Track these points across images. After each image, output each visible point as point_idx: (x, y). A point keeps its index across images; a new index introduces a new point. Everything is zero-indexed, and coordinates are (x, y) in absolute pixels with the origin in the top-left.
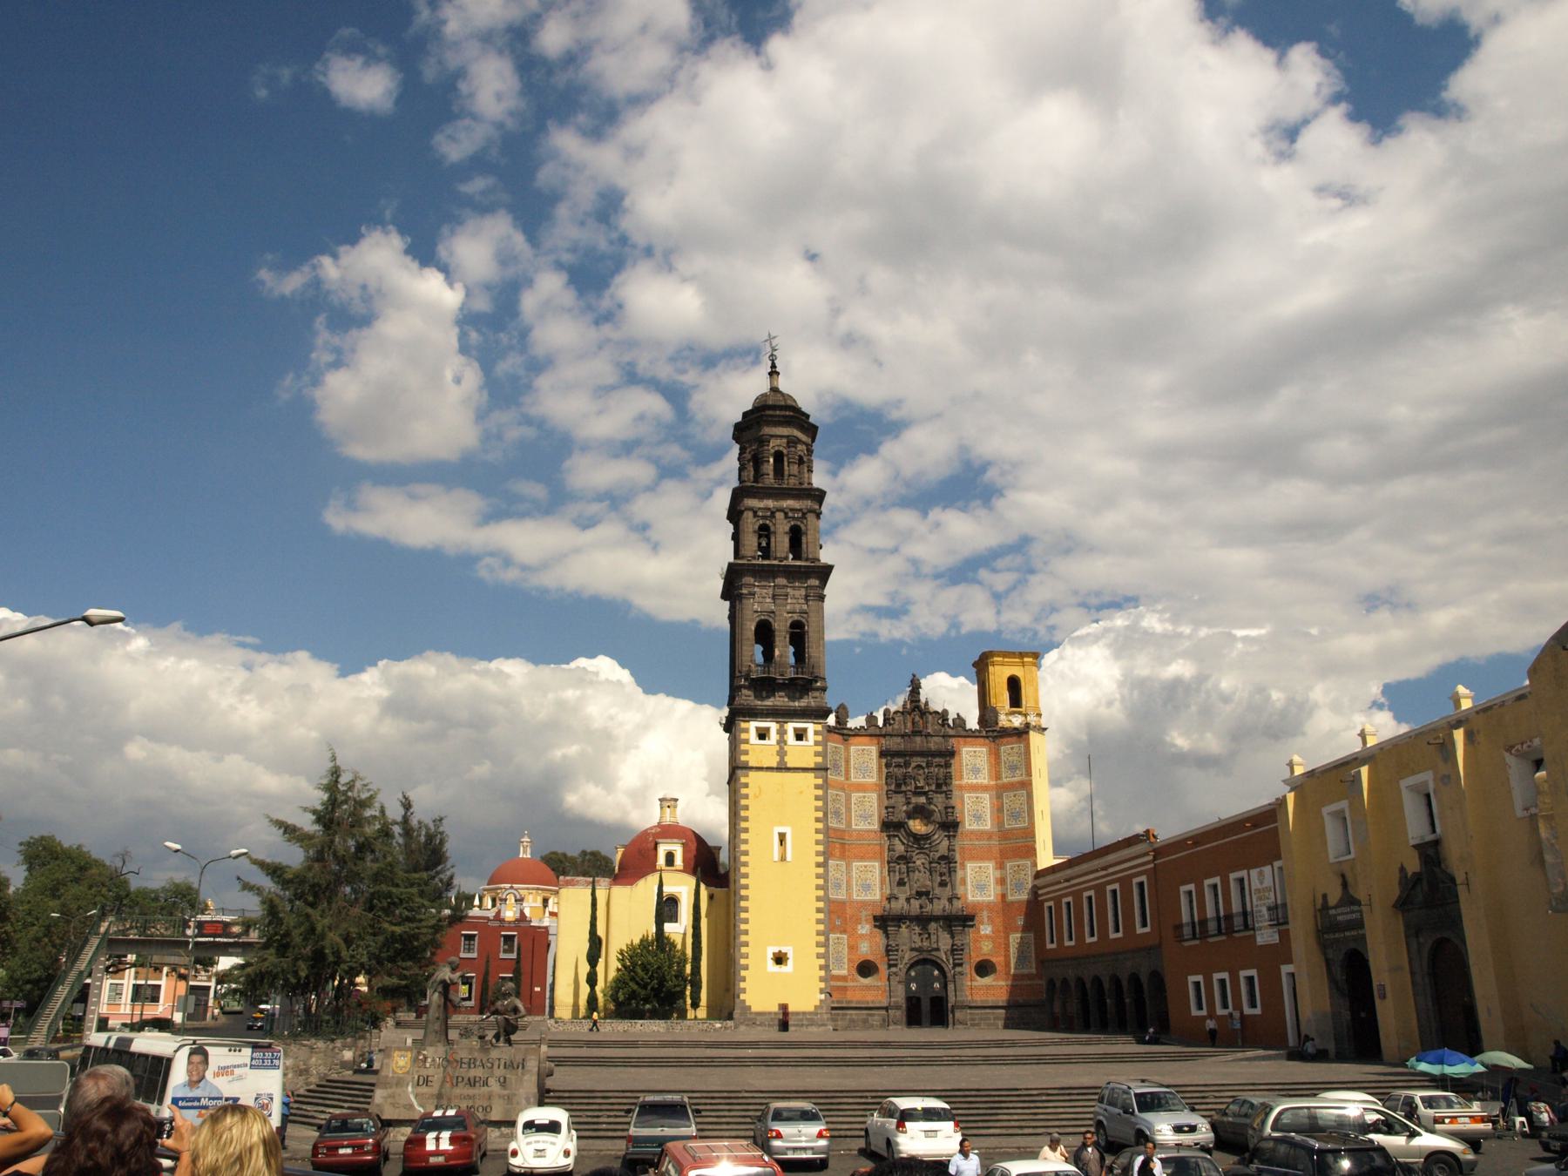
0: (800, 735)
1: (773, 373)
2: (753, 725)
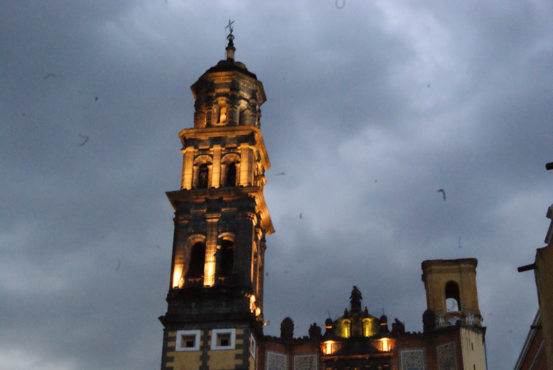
0: (224, 340)
1: (231, 47)
2: (179, 334)
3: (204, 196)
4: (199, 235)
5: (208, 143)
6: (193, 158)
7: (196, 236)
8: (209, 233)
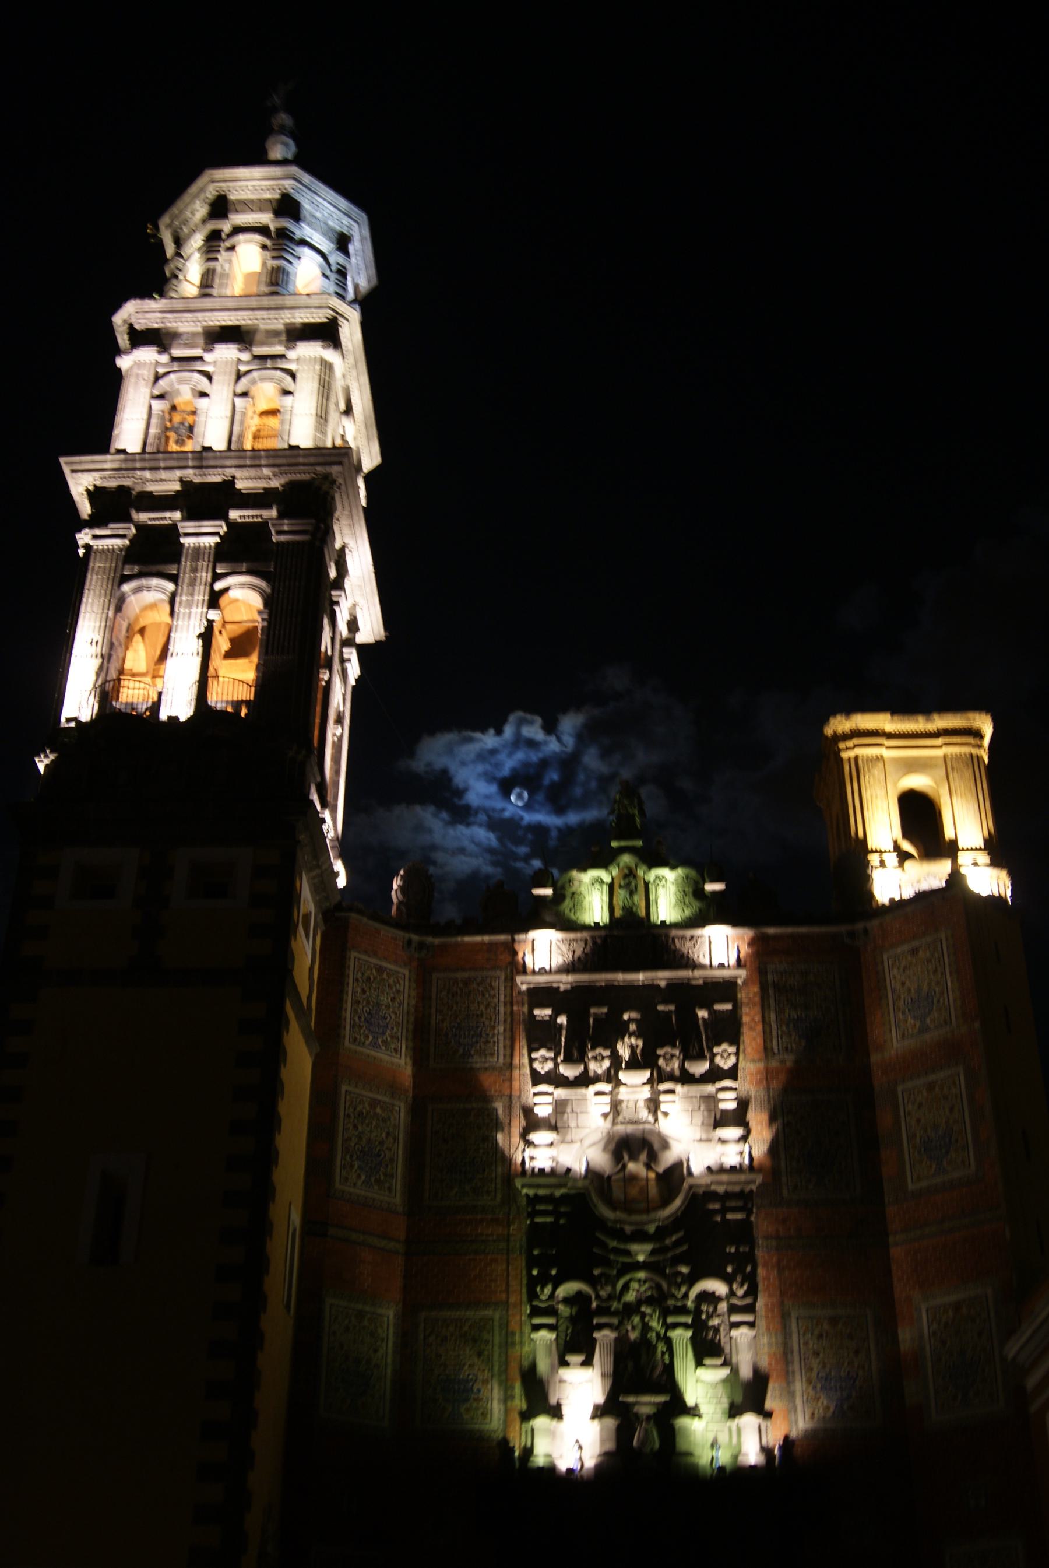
3: (178, 473)
4: (155, 581)
5: (201, 341)
6: (152, 378)
7: (144, 582)
8: (186, 577)
